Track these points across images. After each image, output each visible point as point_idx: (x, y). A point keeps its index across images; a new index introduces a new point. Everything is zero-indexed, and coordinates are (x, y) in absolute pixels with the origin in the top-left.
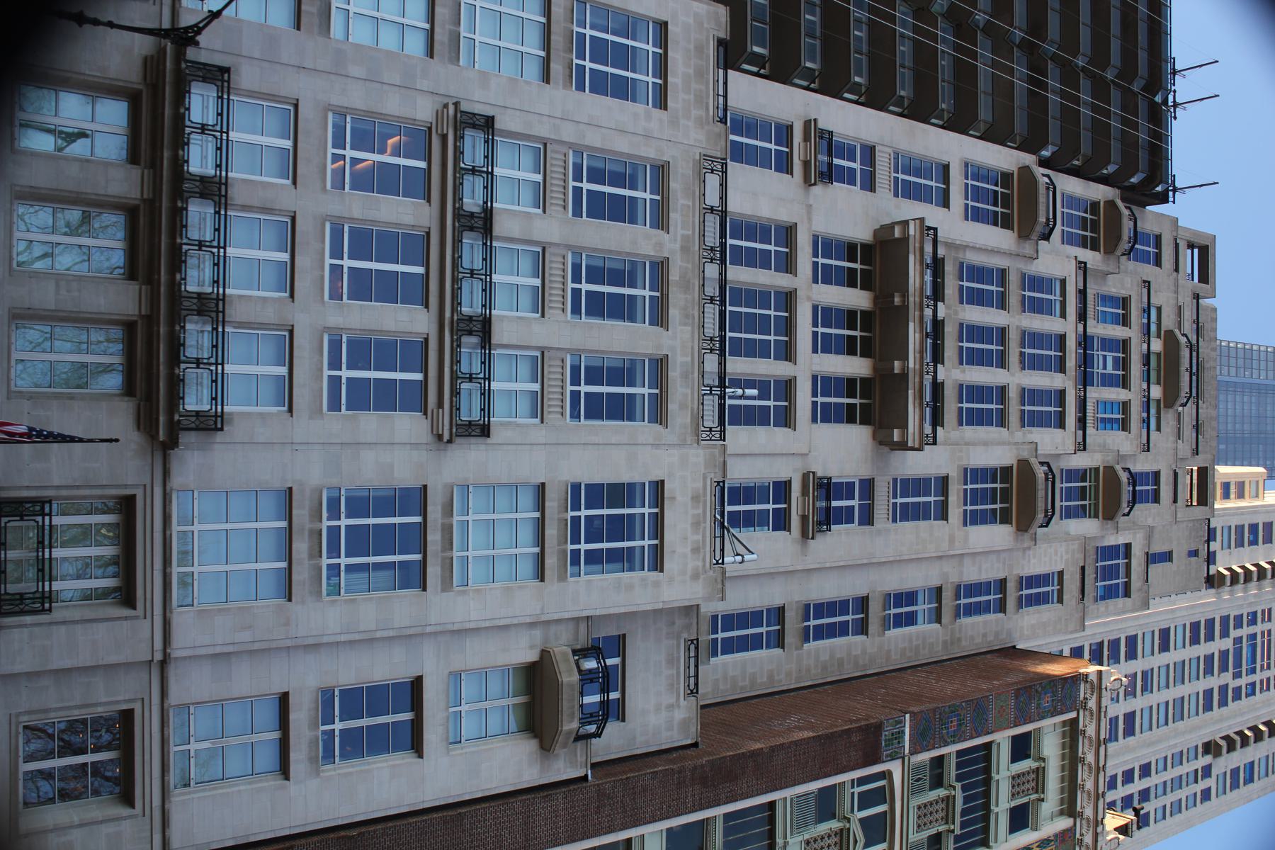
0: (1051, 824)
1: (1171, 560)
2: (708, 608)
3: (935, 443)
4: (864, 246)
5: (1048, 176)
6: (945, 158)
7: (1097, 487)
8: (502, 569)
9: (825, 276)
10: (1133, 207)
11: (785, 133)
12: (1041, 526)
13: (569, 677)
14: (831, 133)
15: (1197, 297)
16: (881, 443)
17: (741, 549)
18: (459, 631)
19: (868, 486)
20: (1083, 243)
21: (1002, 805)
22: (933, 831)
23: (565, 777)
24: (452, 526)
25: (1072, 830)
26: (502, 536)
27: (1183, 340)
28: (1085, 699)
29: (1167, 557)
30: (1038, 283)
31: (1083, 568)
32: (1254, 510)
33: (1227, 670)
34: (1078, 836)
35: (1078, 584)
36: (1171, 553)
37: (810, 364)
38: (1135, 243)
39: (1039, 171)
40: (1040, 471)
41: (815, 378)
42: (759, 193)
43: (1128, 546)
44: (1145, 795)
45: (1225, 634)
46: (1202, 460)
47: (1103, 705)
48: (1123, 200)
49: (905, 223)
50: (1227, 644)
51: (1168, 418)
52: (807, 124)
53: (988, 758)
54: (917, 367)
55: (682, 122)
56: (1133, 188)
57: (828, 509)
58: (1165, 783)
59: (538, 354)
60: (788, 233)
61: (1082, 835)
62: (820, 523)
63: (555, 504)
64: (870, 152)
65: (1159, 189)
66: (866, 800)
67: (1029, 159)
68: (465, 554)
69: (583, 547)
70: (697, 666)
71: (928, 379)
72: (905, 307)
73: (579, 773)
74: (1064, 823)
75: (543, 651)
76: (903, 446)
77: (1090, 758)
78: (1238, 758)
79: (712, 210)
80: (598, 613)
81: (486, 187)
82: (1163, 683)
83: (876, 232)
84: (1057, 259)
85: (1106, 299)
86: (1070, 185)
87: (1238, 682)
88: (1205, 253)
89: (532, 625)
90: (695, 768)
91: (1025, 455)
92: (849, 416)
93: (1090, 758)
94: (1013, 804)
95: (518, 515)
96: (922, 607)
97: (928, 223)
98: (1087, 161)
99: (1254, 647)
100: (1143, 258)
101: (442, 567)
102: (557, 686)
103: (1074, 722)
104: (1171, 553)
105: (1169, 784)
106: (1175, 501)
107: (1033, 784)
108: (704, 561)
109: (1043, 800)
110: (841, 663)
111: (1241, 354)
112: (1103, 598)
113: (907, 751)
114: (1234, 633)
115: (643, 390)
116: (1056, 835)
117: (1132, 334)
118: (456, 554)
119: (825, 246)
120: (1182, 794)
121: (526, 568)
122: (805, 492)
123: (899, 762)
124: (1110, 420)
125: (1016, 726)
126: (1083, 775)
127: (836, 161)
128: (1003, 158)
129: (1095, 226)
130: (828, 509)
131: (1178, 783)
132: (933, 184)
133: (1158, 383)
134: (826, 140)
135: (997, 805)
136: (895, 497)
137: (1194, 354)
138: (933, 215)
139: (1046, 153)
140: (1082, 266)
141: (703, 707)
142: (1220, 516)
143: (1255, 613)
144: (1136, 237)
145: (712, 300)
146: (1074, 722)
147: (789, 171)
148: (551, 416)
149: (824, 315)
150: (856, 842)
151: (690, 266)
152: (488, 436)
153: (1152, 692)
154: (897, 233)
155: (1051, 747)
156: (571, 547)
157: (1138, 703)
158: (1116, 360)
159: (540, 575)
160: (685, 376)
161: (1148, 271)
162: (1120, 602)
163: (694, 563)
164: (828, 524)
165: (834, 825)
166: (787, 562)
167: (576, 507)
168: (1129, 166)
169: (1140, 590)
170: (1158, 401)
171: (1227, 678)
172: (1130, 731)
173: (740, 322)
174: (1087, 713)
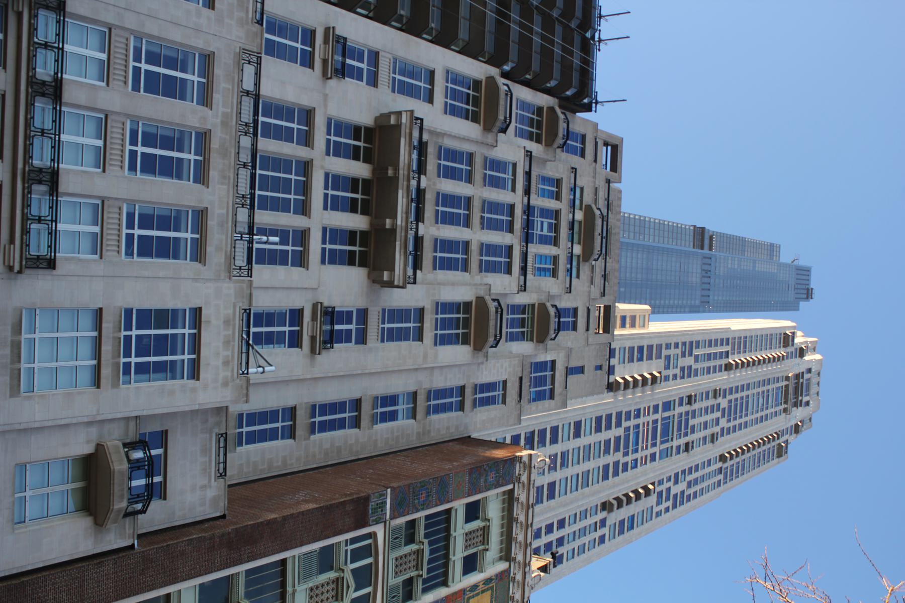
0: (493, 567)
1: (583, 372)
2: (236, 408)
3: (415, 283)
4: (367, 129)
5: (507, 85)
6: (432, 66)
7: (533, 319)
8: (63, 378)
9: (337, 150)
10: (567, 113)
11: (309, 36)
12: (492, 347)
13: (120, 466)
14: (345, 39)
15: (608, 182)
16: (374, 282)
17: (262, 362)
18: (25, 430)
19: (363, 314)
20: (530, 137)
21: (458, 554)
22: (407, 576)
23: (115, 547)
24: (20, 342)
25: (508, 571)
26: (64, 350)
27: (597, 213)
28: (520, 475)
29: (580, 370)
30: (496, 165)
31: (521, 378)
32: (641, 336)
33: (619, 450)
34: (512, 575)
35: (517, 390)
36: (583, 367)
37: (321, 218)
38: (567, 139)
39: (501, 81)
40: (492, 306)
41: (324, 230)
42: (285, 82)
43: (553, 362)
44: (560, 542)
45: (619, 424)
46: (606, 301)
47: (532, 479)
48: (560, 107)
49: (399, 114)
50: (620, 432)
51: (585, 269)
52: (327, 30)
54: (404, 224)
55: (227, 20)
56: (567, 99)
57: (332, 331)
58: (574, 532)
59: (99, 202)
60: (308, 115)
61: (515, 574)
62: (325, 342)
63: (111, 325)
64: (375, 56)
65: (586, 101)
67: (494, 71)
68: (32, 365)
69: (134, 360)
70: (225, 454)
71: (411, 234)
72: (396, 178)
73: (127, 543)
74: (502, 566)
75: (98, 445)
76: (390, 284)
77: (522, 518)
78: (624, 513)
79: (248, 93)
80: (145, 413)
81: (57, 61)
83: (376, 119)
84: (511, 148)
85: (545, 180)
86: (523, 93)
87: (626, 459)
88: (615, 150)
89: (89, 424)
90: (223, 535)
91: (481, 293)
92: (350, 260)
93: (522, 518)
94: (466, 554)
95: (79, 334)
96: (402, 407)
97: (417, 115)
98: (536, 76)
99: (637, 434)
100: (572, 151)
101: (11, 378)
102: (109, 473)
103: (512, 491)
104: (583, 367)
105: (577, 533)
106: (588, 329)
107: (481, 538)
108: (233, 371)
110: (339, 450)
111: (637, 223)
112: (534, 400)
113: (388, 517)
114: (625, 424)
115: (187, 235)
116: (496, 575)
117: (562, 206)
118: (24, 366)
119: (337, 127)
120: (585, 540)
121: (85, 377)
122: (314, 318)
123: (382, 525)
124: (544, 269)
125: (469, 496)
127: (348, 61)
128: (474, 69)
129: (539, 127)
130: (332, 331)
131: (583, 532)
132: (422, 84)
133: (579, 243)
134: (342, 44)
135: (454, 555)
136: (383, 323)
137: (605, 223)
138: (420, 108)
139: (507, 68)
140: (529, 154)
141: (230, 486)
142: (618, 340)
143: (639, 410)
144: (568, 135)
145: (245, 165)
146: (512, 491)
147: (311, 66)
148: (109, 253)
149: (334, 181)
151: (228, 137)
152: (54, 268)
154: (393, 121)
155: (494, 511)
156: (123, 360)
157: (557, 476)
158: (550, 225)
159: (97, 382)
160: (221, 225)
161: (575, 160)
162: (547, 403)
163: (224, 373)
164: (332, 343)
165: (332, 575)
166: (298, 373)
167: (128, 327)
168: (565, 83)
169: (560, 394)
170: (579, 256)
171: (619, 456)
172: (551, 496)
173: (266, 183)
174: (521, 485)
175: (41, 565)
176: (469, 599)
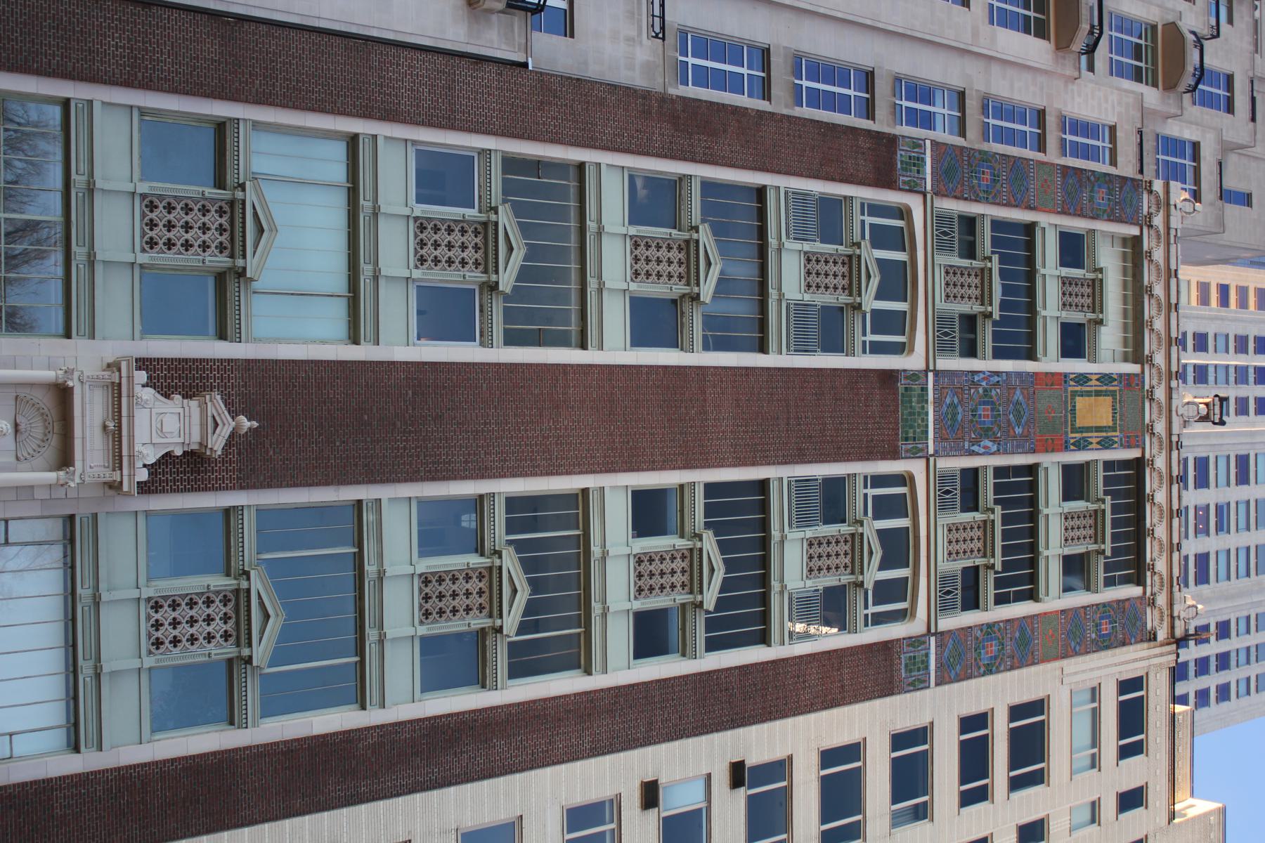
28: (1150, 214)
34: (1147, 387)
35: (1135, 149)
47: (1173, 225)
53: (1033, 486)
58: (1248, 649)
66: (884, 507)
77: (1159, 290)
82: (1242, 524)
105: (1253, 650)
106: (1253, 119)
109: (1101, 322)
113: (929, 187)
125: (1064, 212)
126: (1149, 309)
146: (1137, 240)
150: (869, 277)
153: (1229, 532)
155: (1109, 260)
157: (1212, 543)
172: (1203, 578)
175: (391, 36)
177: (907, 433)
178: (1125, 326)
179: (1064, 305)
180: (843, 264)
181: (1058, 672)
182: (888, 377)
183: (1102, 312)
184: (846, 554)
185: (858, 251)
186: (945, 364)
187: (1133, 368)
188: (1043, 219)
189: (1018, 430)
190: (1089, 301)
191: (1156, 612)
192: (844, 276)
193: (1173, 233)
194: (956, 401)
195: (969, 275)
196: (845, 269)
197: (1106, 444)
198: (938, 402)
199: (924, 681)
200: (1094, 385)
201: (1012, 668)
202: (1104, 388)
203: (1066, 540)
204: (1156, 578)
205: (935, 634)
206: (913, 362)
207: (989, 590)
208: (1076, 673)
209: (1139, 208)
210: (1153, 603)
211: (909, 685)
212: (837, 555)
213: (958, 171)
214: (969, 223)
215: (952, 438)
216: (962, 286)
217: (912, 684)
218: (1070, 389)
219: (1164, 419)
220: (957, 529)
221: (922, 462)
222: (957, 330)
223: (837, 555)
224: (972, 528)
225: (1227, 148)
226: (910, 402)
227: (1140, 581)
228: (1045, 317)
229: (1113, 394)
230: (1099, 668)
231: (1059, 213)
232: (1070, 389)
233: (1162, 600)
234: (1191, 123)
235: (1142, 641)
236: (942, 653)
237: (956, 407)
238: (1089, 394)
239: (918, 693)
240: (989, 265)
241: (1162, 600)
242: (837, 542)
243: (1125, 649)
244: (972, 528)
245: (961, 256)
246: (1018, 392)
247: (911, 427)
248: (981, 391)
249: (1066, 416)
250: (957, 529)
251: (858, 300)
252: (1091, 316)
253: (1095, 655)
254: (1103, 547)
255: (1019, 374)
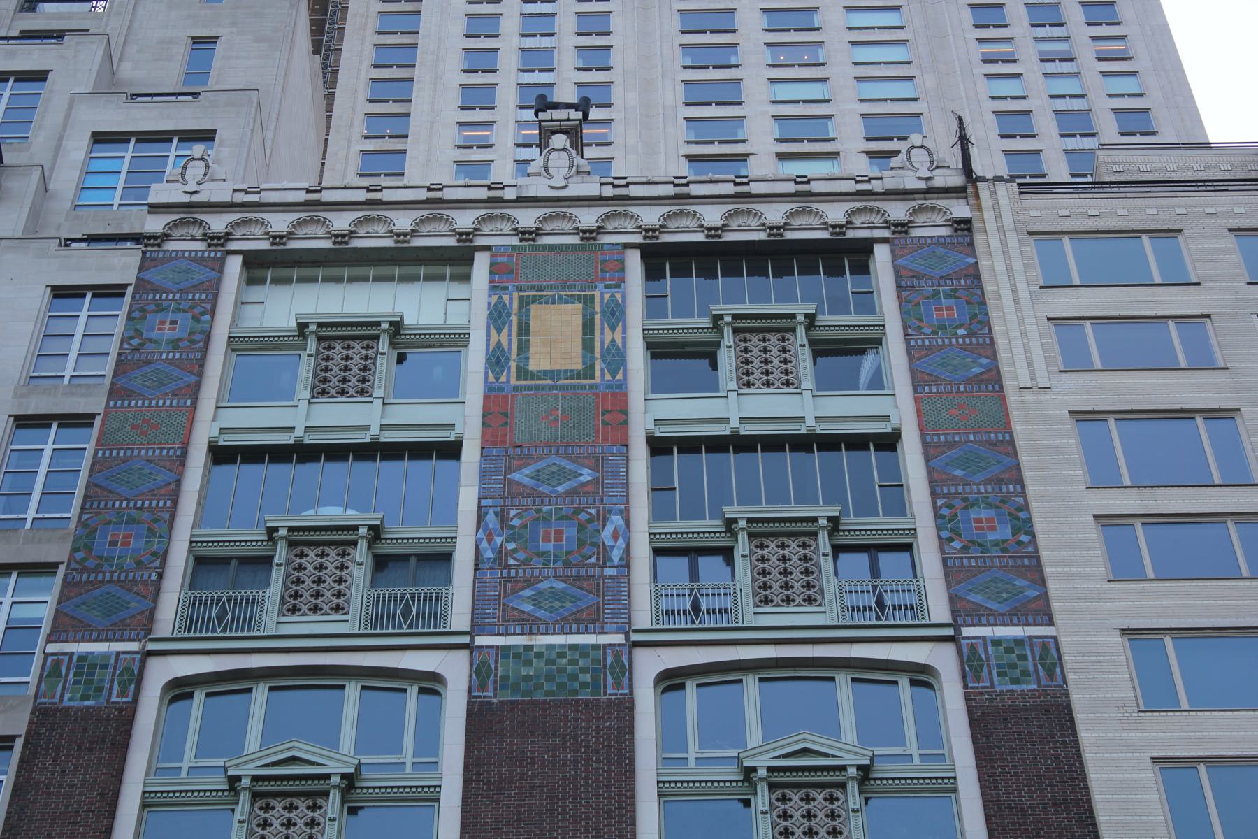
28: (205, 237)
47: (226, 197)
93: (403, 221)
104: (196, 40)
109: (397, 327)
113: (134, 646)
126: (375, 239)
174: (238, 233)
176: (523, 373)
177: (584, 685)
178: (404, 279)
179: (362, 392)
180: (267, 808)
181: (1028, 396)
182: (480, 719)
183: (378, 324)
184: (807, 799)
185: (246, 782)
186: (460, 616)
187: (481, 264)
188: (205, 431)
189: (586, 475)
190: (357, 346)
191: (920, 219)
192: (291, 808)
193: (240, 198)
194: (528, 593)
195: (300, 568)
196: (278, 805)
197: (615, 314)
198: (530, 625)
199: (1045, 647)
200: (508, 339)
201: (1020, 481)
202: (514, 319)
203: (788, 384)
204: (858, 220)
205: (956, 626)
206: (454, 669)
207: (878, 524)
208: (1030, 363)
209: (195, 258)
210: (902, 227)
211: (1051, 675)
212: (809, 815)
213: (103, 588)
214: (205, 564)
215: (598, 596)
216: (319, 581)
217: (1051, 675)
218: (513, 382)
219: (574, 211)
220: (765, 587)
221: (641, 655)
222: (398, 590)
223: (809, 815)
224: (763, 559)
225: (109, 83)
226: (527, 678)
227: (863, 250)
228: (383, 427)
229: (525, 303)
230: (1021, 320)
231: (195, 404)
232: (513, 382)
233: (897, 211)
234: (58, 148)
235: (971, 244)
236: (991, 612)
237: (540, 593)
238: (524, 347)
239: (1067, 659)
240: (283, 532)
241: (897, 211)
242: (785, 815)
243: (985, 275)
244: (763, 559)
245: (267, 583)
246: (516, 476)
247: (573, 677)
248: (511, 546)
249: (563, 388)
250: (765, 587)
251: (335, 780)
252: (384, 343)
253: (997, 328)
254: (800, 318)
255: (484, 475)
